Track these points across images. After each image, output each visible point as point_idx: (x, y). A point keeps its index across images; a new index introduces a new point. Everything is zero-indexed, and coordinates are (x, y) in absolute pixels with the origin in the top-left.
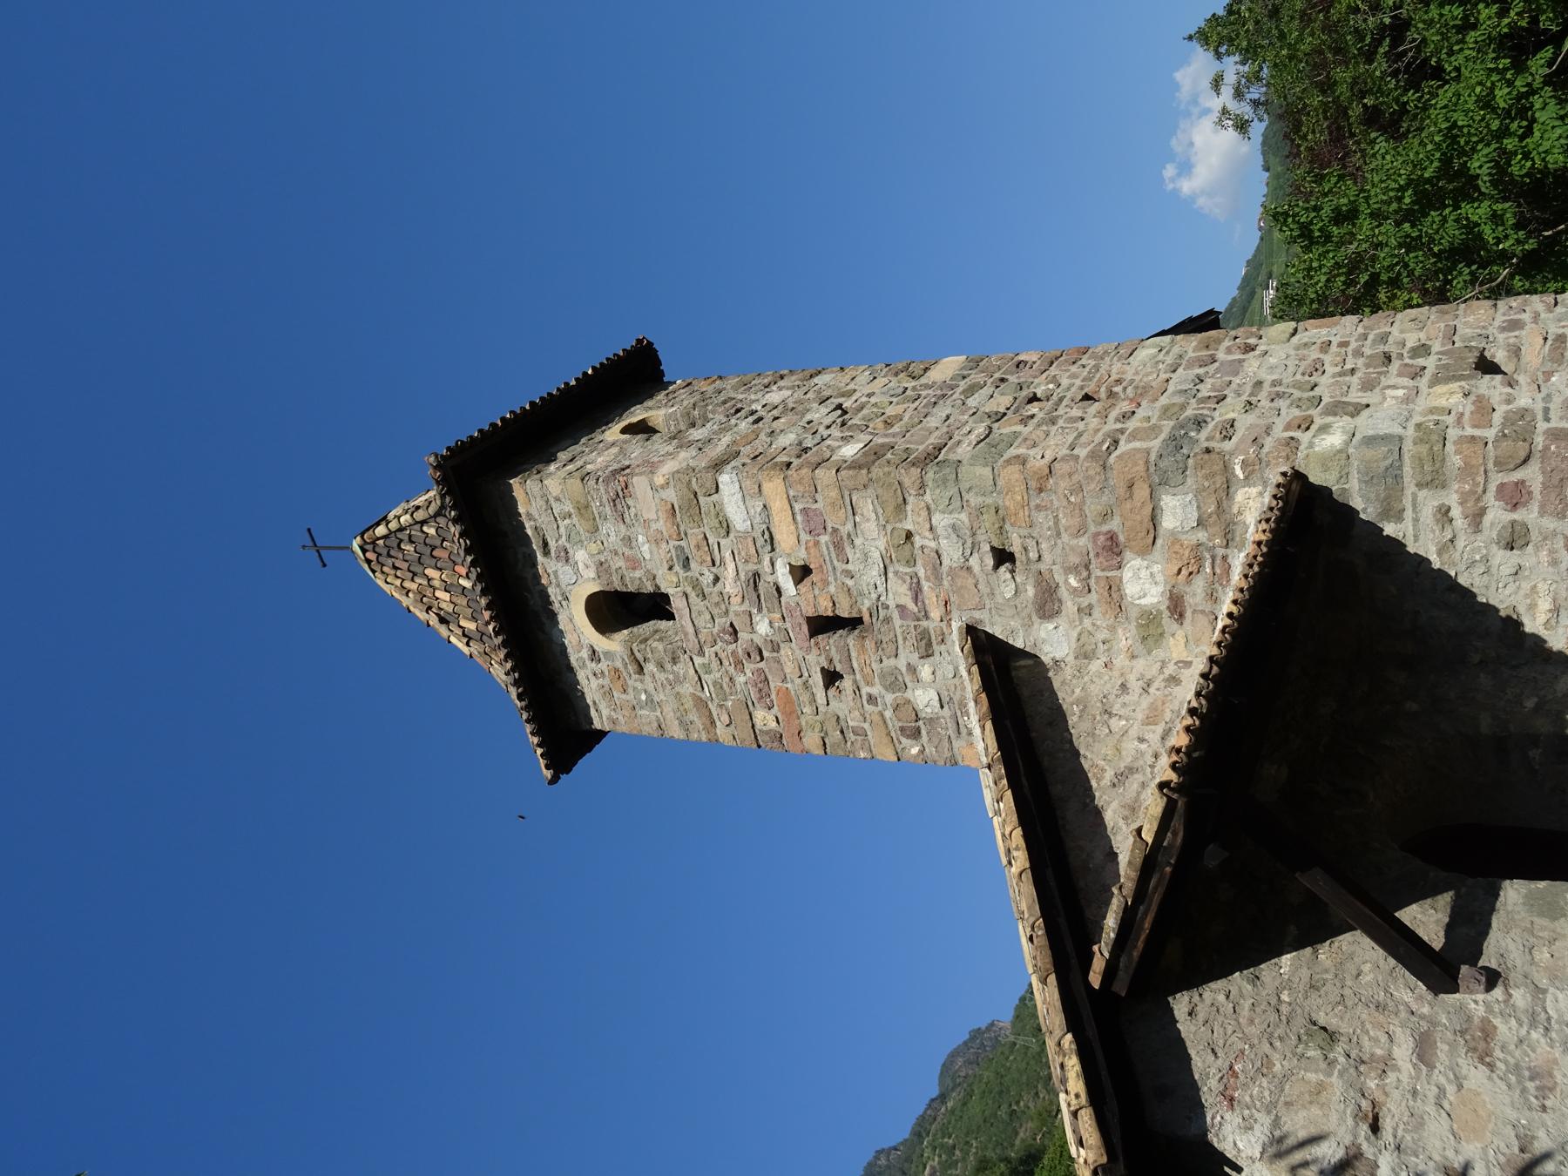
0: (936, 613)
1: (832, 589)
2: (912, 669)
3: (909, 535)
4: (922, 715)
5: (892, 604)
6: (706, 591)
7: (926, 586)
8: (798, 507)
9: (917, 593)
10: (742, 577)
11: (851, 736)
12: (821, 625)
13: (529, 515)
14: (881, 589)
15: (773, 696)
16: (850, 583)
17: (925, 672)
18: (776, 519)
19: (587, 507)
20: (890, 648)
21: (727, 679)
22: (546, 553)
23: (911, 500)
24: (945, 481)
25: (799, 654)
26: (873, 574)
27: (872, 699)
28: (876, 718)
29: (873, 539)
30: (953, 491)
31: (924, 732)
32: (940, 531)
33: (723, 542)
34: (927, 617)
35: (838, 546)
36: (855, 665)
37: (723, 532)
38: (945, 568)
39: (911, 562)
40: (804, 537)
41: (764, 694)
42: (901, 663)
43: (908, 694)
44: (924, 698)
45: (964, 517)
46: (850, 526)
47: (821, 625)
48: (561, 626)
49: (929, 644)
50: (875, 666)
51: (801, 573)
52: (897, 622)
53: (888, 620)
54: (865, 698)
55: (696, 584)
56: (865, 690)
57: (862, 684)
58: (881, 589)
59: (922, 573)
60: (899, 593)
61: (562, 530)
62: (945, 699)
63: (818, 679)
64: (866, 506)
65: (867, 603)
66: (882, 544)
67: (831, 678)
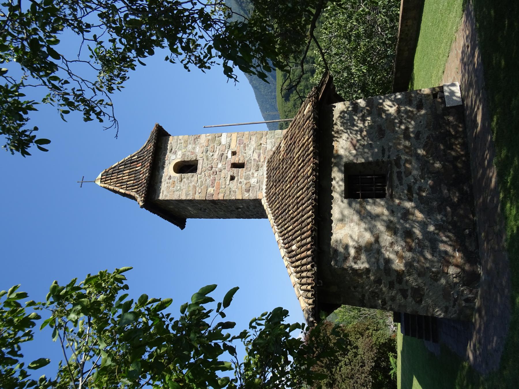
0: (262, 160)
1: (240, 156)
2: (253, 174)
3: (261, 144)
4: (252, 185)
5: (252, 159)
6: (209, 158)
7: (261, 154)
8: (238, 139)
9: (259, 156)
10: (219, 154)
11: (232, 193)
12: (235, 165)
13: (171, 143)
14: (251, 155)
15: (215, 184)
16: (244, 155)
17: (255, 175)
18: (232, 141)
19: (187, 141)
20: (249, 169)
21: (205, 180)
22: (171, 152)
23: (263, 137)
24: (272, 133)
25: (226, 172)
26: (251, 152)
27: (240, 183)
28: (240, 187)
29: (253, 144)
30: (273, 135)
31: (251, 190)
32: (268, 143)
33: (218, 147)
34: (260, 161)
35: (245, 147)
36: (239, 174)
37: (219, 144)
38: (267, 151)
39: (260, 149)
40: (237, 145)
41: (213, 183)
42: (250, 173)
43: (250, 181)
44: (253, 181)
45: (274, 140)
46: (249, 142)
47: (235, 165)
48: (164, 171)
49: (258, 168)
50: (244, 174)
51: (234, 153)
52: (253, 163)
53: (251, 163)
54: (239, 182)
55: (207, 156)
56: (240, 180)
57: (239, 179)
58: (251, 155)
59: (261, 152)
60: (256, 156)
61: (178, 147)
62: (258, 181)
63: (229, 178)
64: (254, 138)
65: (247, 159)
66: (254, 146)
67: (232, 178)
